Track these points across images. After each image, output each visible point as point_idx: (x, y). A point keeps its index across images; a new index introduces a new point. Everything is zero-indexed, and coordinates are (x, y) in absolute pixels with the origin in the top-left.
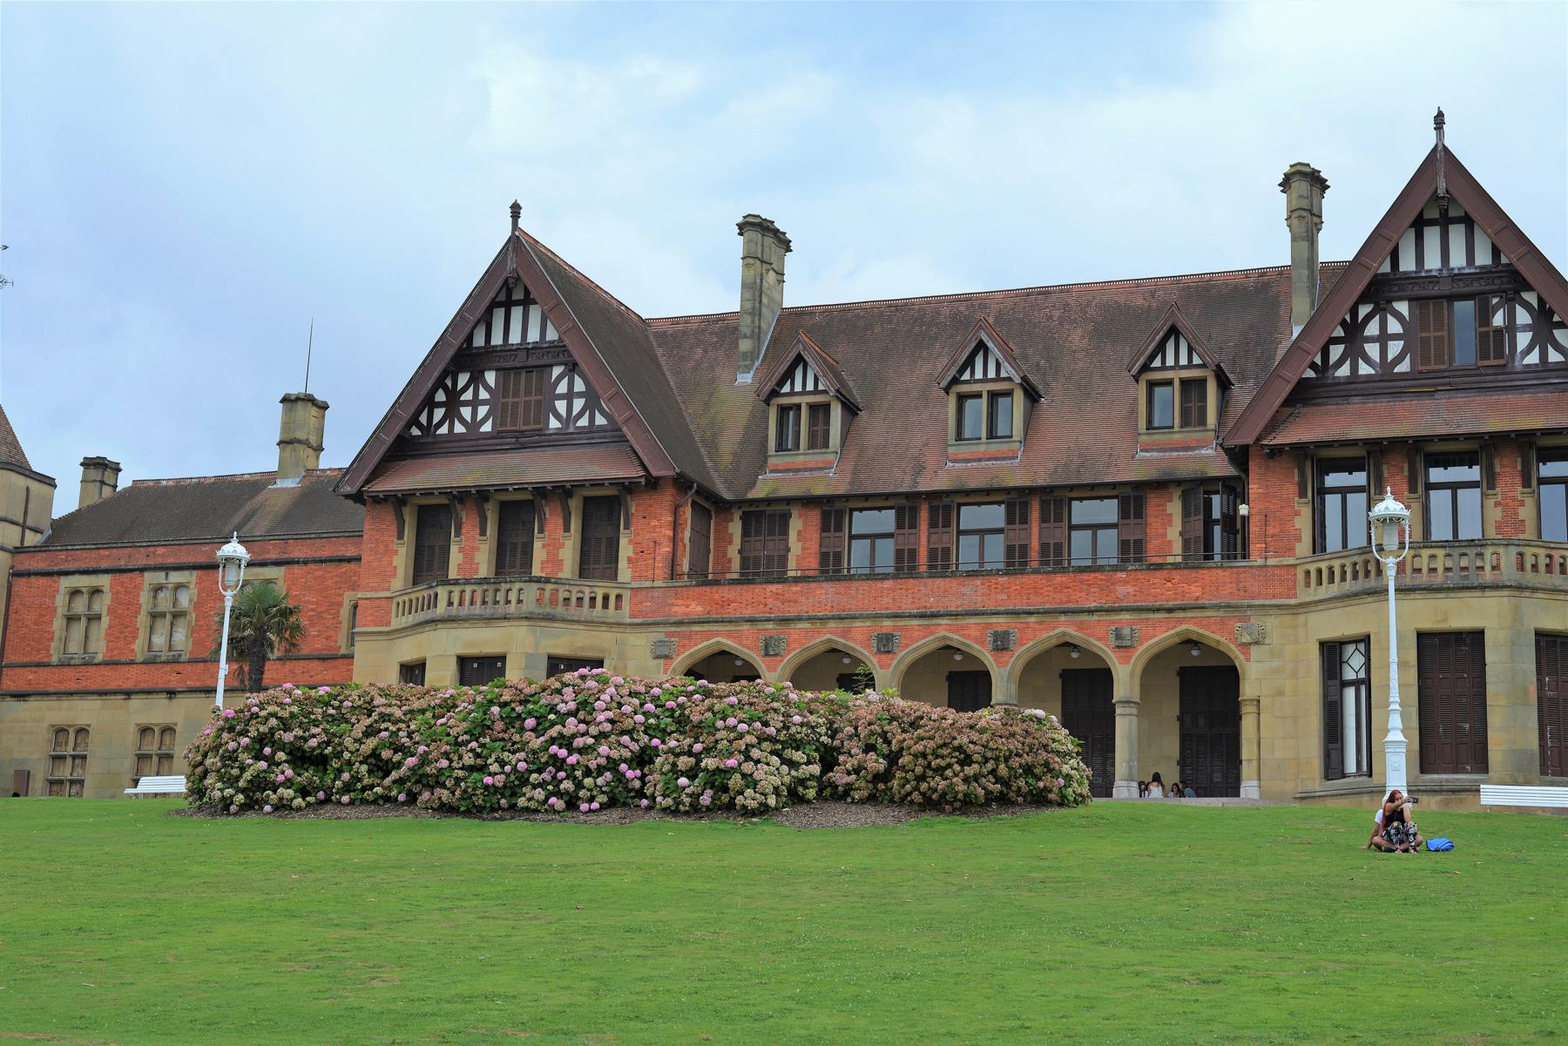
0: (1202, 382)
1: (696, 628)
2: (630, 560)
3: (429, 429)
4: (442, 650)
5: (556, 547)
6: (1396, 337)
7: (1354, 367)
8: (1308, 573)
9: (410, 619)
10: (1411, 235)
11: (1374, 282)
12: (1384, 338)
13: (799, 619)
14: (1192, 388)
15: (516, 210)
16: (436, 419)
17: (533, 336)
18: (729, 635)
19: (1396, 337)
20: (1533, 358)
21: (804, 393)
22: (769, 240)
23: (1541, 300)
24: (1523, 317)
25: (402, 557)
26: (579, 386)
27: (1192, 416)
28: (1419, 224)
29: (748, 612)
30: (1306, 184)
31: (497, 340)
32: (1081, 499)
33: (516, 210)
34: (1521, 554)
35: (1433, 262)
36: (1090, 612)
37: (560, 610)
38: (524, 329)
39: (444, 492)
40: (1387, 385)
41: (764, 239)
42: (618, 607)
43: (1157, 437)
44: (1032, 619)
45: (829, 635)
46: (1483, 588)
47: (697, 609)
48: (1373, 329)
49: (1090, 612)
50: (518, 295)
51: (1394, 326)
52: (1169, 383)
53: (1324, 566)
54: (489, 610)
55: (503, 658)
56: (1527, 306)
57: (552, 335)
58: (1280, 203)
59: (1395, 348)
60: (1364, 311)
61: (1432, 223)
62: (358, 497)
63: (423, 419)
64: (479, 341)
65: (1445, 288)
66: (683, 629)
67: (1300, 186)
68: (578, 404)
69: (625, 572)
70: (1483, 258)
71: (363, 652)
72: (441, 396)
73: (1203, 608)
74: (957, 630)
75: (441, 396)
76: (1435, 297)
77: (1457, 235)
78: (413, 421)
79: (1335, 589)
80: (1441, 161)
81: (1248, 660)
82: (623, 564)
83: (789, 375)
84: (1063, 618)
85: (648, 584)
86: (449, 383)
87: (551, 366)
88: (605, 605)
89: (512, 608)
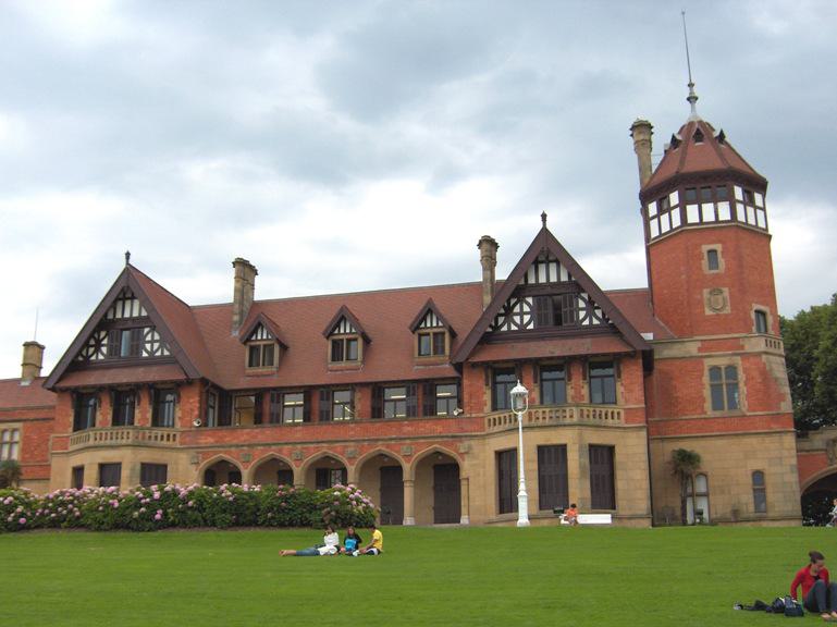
0: (443, 334)
3: (87, 358)
4: (90, 461)
5: (143, 412)
6: (527, 313)
7: (509, 327)
9: (76, 447)
10: (533, 267)
11: (518, 288)
14: (269, 348)
15: (128, 255)
16: (90, 353)
17: (135, 314)
18: (225, 453)
19: (527, 313)
20: (586, 323)
21: (262, 339)
22: (247, 269)
23: (590, 298)
24: (582, 304)
25: (72, 419)
26: (157, 337)
27: (438, 350)
28: (536, 263)
29: (235, 442)
30: (489, 245)
31: (119, 316)
32: (389, 388)
33: (128, 255)
34: (582, 410)
35: (542, 280)
36: (391, 439)
37: (146, 441)
38: (133, 310)
39: (93, 387)
40: (522, 335)
41: (245, 271)
42: (174, 440)
43: (423, 359)
45: (272, 452)
46: (565, 425)
47: (211, 440)
48: (517, 309)
49: (391, 439)
50: (129, 295)
51: (526, 309)
52: (428, 334)
53: (497, 417)
54: (114, 442)
55: (119, 464)
56: (583, 299)
57: (144, 313)
58: (477, 253)
59: (527, 318)
60: (513, 301)
61: (542, 262)
62: (53, 389)
63: (84, 353)
64: (110, 316)
65: (549, 291)
67: (485, 245)
68: (156, 345)
69: (178, 425)
70: (564, 278)
71: (56, 463)
72: (92, 342)
74: (331, 449)
75: (92, 342)
76: (543, 294)
77: (553, 267)
78: (80, 353)
79: (501, 428)
80: (545, 234)
83: (255, 332)
86: (96, 336)
87: (144, 328)
88: (168, 440)
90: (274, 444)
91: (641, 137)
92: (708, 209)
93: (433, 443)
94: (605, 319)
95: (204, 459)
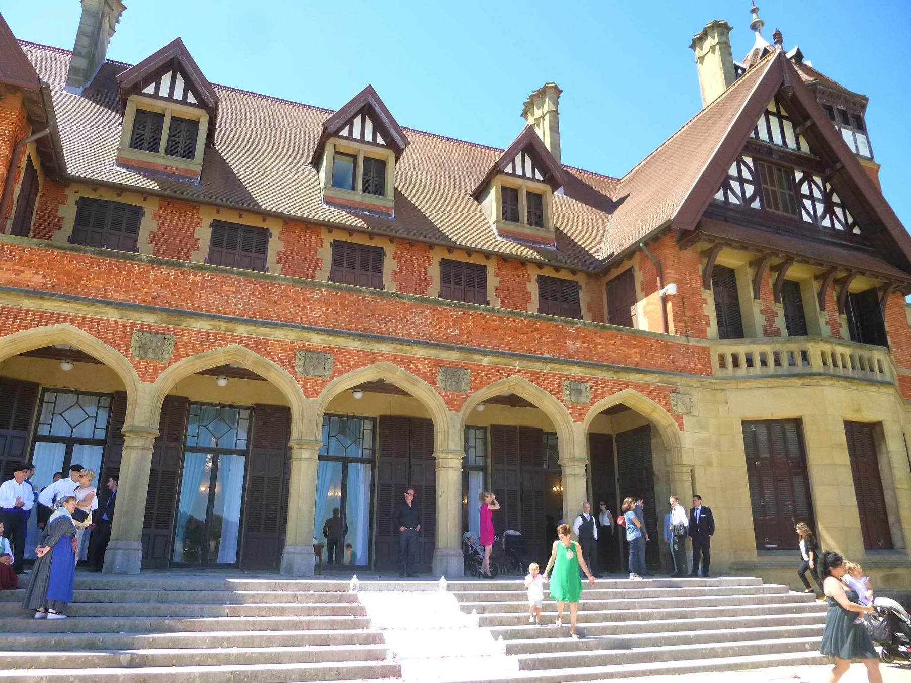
1: (29, 304)
8: (722, 358)
12: (742, 181)
13: (195, 315)
18: (82, 323)
29: (120, 296)
44: (486, 361)
47: (33, 278)
49: (544, 360)
73: (645, 372)
81: (682, 429)
84: (517, 364)
90: (246, 322)
91: (724, 39)
93: (626, 384)
94: (849, 227)
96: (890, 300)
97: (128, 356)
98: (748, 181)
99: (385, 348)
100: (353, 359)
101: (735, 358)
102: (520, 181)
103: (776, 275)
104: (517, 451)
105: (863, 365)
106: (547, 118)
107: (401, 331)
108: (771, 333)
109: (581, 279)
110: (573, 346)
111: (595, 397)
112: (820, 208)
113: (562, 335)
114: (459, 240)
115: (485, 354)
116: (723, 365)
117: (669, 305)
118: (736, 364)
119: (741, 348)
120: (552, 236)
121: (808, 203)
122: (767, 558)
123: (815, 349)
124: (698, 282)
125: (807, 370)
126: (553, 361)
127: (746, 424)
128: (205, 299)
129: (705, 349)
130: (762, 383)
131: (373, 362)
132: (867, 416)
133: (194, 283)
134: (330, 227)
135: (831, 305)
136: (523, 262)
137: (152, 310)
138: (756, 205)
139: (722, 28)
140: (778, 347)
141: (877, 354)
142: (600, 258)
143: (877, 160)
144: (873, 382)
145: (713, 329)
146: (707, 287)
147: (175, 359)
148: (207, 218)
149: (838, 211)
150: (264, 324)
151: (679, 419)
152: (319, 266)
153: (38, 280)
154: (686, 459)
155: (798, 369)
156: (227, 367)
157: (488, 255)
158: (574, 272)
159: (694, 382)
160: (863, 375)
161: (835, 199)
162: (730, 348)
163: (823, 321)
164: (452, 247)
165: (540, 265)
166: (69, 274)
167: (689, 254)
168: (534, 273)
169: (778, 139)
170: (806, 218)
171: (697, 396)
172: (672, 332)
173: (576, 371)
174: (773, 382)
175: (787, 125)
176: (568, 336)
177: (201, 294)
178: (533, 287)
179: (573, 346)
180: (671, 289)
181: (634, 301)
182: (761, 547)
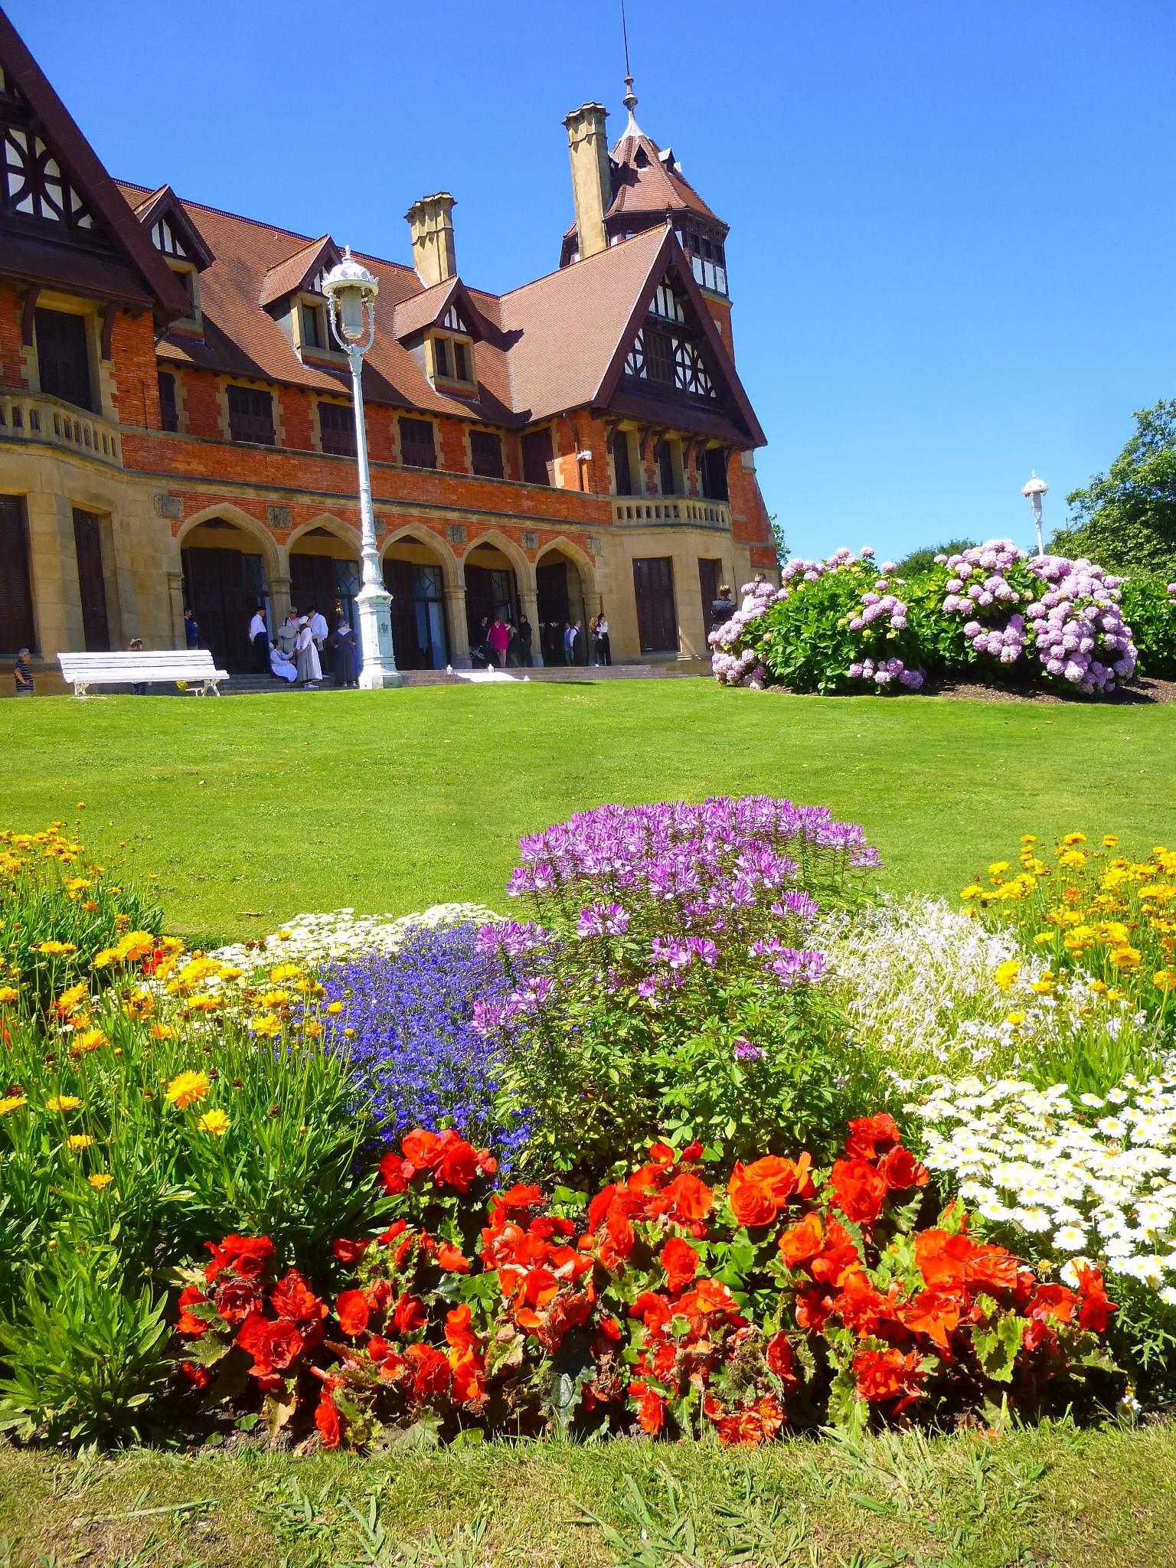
1: (202, 489)
2: (114, 397)
8: (619, 510)
13: (300, 492)
18: (236, 502)
29: (253, 479)
37: (73, 445)
44: (474, 518)
47: (198, 467)
66: (186, 487)
73: (571, 523)
82: (107, 402)
84: (493, 520)
85: (141, 430)
89: (27, 432)
90: (333, 496)
92: (708, 266)
93: (559, 533)
95: (189, 511)
96: (733, 457)
97: (268, 526)
98: (638, 352)
99: (415, 512)
100: (397, 521)
101: (629, 510)
102: (448, 334)
103: (656, 439)
104: (488, 584)
105: (712, 516)
106: (442, 234)
107: (422, 498)
108: (652, 489)
109: (502, 434)
110: (526, 504)
111: (542, 544)
112: (689, 373)
113: (518, 496)
114: (419, 404)
115: (474, 513)
116: (620, 517)
117: (585, 467)
118: (629, 516)
119: (632, 503)
120: (476, 389)
121: (680, 370)
122: (648, 657)
123: (683, 504)
124: (603, 447)
125: (677, 521)
126: (515, 517)
127: (635, 561)
128: (304, 479)
129: (608, 504)
130: (646, 530)
131: (409, 522)
132: (712, 555)
133: (294, 466)
134: (320, 392)
135: (692, 463)
136: (461, 420)
137: (275, 489)
138: (643, 375)
139: (599, 115)
140: (659, 503)
141: (722, 508)
142: (516, 410)
143: (731, 298)
144: (718, 529)
145: (613, 487)
146: (610, 452)
147: (295, 526)
148: (223, 384)
149: (701, 376)
150: (344, 497)
151: (592, 559)
152: (312, 428)
153: (202, 468)
154: (597, 589)
155: (669, 520)
156: (319, 529)
157: (436, 414)
158: (498, 428)
159: (601, 530)
160: (712, 524)
161: (700, 365)
162: (625, 502)
163: (685, 476)
164: (411, 408)
165: (474, 422)
166: (218, 463)
167: (598, 423)
168: (467, 428)
169: (662, 311)
170: (679, 385)
171: (604, 540)
172: (587, 490)
173: (529, 524)
174: (655, 530)
175: (669, 292)
176: (522, 497)
177: (300, 474)
178: (467, 441)
179: (526, 504)
180: (587, 454)
181: (551, 458)
182: (643, 651)
